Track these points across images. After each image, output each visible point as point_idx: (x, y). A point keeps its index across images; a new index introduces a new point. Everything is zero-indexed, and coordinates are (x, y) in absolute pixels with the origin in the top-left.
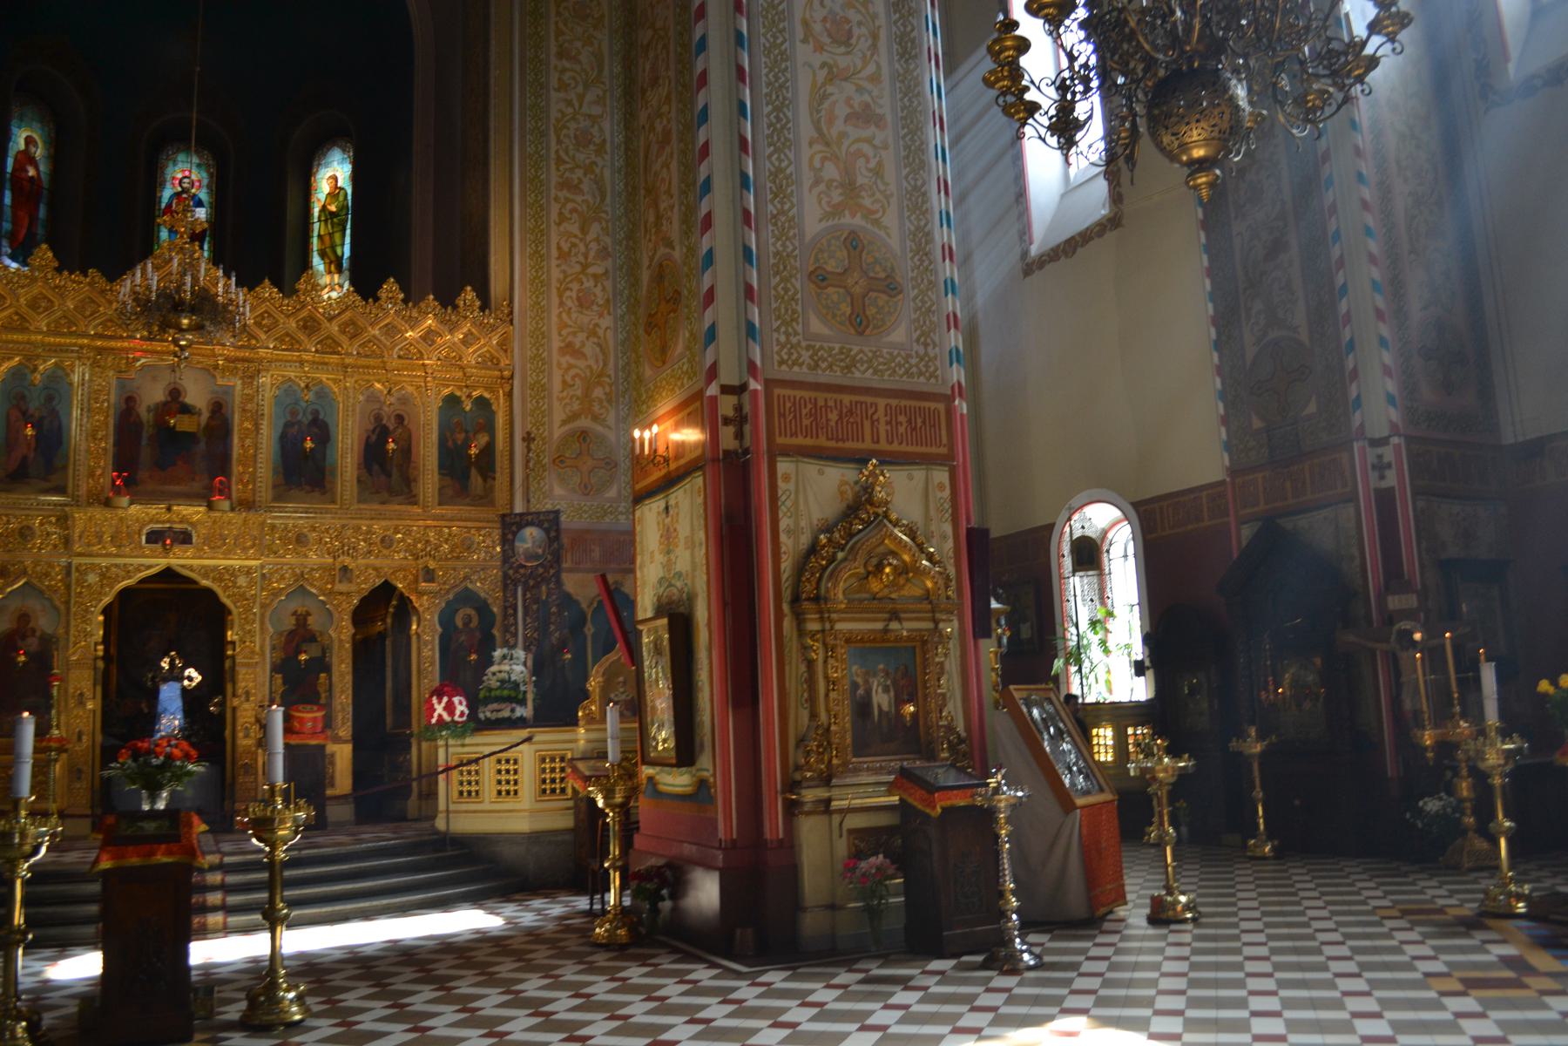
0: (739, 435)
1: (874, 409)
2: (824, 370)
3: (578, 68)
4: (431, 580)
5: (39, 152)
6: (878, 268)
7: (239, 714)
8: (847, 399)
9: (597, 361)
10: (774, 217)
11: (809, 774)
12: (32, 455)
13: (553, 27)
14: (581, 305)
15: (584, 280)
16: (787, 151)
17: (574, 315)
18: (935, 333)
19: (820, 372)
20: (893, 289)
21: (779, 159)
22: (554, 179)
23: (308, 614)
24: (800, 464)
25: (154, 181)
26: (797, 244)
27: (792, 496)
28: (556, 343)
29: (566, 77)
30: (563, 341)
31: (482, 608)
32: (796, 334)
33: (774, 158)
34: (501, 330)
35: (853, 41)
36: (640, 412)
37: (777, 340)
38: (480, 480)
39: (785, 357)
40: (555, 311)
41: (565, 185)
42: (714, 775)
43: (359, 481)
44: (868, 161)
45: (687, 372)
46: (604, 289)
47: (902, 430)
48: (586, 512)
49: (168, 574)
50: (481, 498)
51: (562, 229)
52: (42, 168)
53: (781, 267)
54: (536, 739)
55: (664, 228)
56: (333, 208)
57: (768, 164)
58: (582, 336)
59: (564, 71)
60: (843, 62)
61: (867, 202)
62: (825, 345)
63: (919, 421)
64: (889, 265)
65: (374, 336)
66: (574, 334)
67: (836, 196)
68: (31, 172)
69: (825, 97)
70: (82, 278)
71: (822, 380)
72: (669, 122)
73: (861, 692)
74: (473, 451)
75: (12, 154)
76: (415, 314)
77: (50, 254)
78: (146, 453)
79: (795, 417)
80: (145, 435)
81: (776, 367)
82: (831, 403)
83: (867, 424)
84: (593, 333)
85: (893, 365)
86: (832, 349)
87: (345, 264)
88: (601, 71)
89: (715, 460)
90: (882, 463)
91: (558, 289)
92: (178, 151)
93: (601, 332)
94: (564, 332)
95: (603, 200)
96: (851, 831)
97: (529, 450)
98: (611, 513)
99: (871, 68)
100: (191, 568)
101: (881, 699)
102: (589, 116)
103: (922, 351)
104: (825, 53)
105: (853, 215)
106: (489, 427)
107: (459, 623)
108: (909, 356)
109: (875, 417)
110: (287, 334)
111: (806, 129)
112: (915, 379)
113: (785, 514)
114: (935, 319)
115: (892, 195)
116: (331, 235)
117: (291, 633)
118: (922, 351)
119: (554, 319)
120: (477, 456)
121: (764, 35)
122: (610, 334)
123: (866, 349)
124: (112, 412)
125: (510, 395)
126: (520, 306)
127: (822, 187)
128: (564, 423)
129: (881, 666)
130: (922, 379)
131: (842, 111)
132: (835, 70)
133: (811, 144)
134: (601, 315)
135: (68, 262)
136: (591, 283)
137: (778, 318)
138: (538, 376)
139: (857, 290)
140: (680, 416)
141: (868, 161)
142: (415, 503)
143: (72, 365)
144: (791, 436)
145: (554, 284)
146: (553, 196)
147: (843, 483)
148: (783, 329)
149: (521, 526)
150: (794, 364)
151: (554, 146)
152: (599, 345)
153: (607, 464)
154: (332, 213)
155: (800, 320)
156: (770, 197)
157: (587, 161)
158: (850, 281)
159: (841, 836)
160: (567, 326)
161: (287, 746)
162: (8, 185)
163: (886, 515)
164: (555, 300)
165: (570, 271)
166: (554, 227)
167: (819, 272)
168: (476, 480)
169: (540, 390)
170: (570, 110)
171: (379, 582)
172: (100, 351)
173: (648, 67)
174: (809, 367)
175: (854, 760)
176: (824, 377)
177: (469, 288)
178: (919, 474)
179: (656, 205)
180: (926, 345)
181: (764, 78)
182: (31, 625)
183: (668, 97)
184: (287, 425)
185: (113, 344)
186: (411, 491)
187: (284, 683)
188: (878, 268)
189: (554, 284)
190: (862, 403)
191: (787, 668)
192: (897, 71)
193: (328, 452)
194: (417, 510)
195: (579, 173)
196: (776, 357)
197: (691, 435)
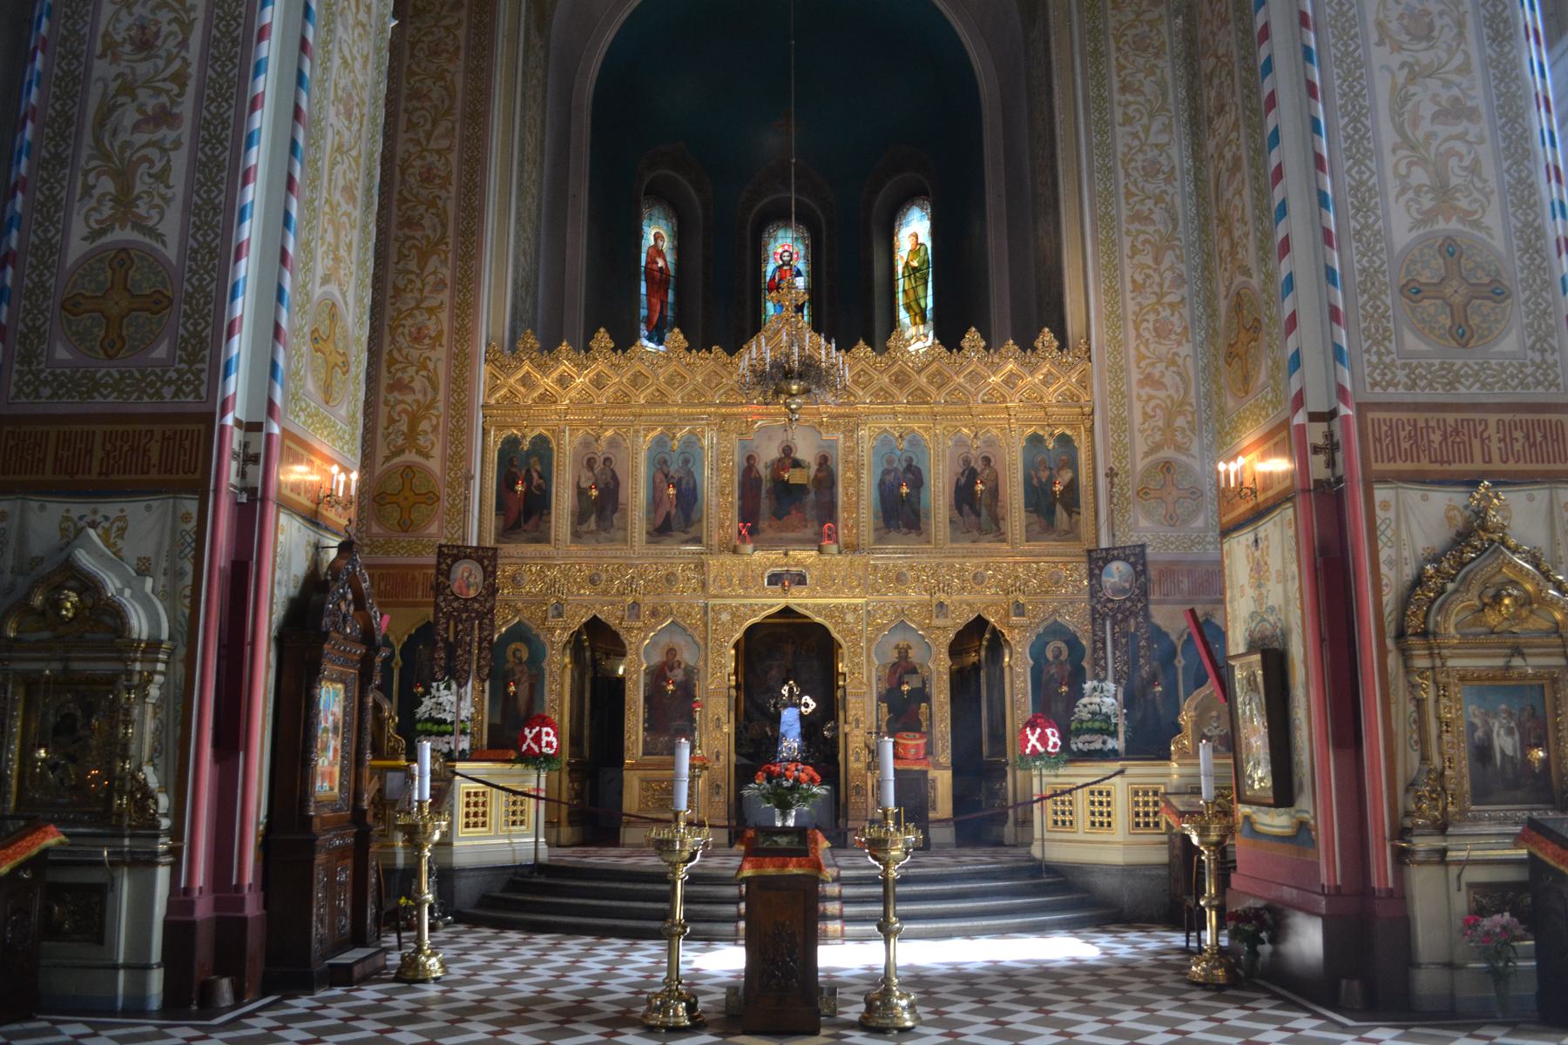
0: (1331, 463)
1: (1483, 427)
2: (1423, 389)
3: (1141, 99)
4: (1022, 614)
5: (666, 245)
6: (1480, 273)
7: (850, 739)
8: (1451, 418)
9: (1177, 391)
10: (1358, 232)
11: (1420, 821)
12: (673, 511)
13: (1114, 63)
14: (1158, 336)
15: (1160, 309)
16: (1367, 162)
17: (1152, 347)
18: (1553, 337)
19: (1418, 391)
20: (1499, 294)
21: (1360, 172)
22: (1125, 213)
23: (909, 647)
24: (1400, 490)
25: (758, 259)
26: (1384, 257)
27: (1393, 525)
28: (1135, 376)
30: (1142, 373)
31: (1073, 642)
32: (1389, 352)
34: (1079, 368)
35: (1436, 34)
36: (1225, 444)
37: (1368, 361)
38: (1065, 515)
39: (1379, 378)
40: (1132, 344)
41: (1137, 217)
42: (1315, 818)
43: (951, 522)
44: (1461, 158)
45: (1271, 401)
47: (1517, 446)
48: (1172, 543)
49: (787, 611)
50: (1067, 533)
51: (1135, 261)
52: (669, 259)
53: (1369, 285)
54: (1128, 772)
55: (1240, 256)
56: (915, 264)
57: (1348, 179)
58: (1161, 366)
59: (1128, 104)
60: (1425, 58)
61: (1463, 203)
62: (1423, 361)
63: (1539, 439)
64: (1493, 268)
65: (959, 384)
66: (1153, 365)
67: (1427, 202)
68: (661, 263)
69: (1407, 98)
70: (707, 355)
71: (1421, 399)
72: (1238, 147)
73: (1479, 733)
74: (1058, 488)
75: (644, 249)
76: (996, 360)
77: (681, 337)
78: (765, 505)
79: (1392, 441)
81: (1368, 390)
82: (1433, 423)
83: (1476, 443)
84: (1172, 363)
85: (1504, 376)
86: (1432, 365)
87: (929, 315)
88: (1165, 99)
89: (1306, 491)
90: (1496, 484)
91: (1134, 322)
92: (778, 228)
93: (1180, 361)
94: (1143, 364)
95: (1175, 228)
96: (1471, 886)
97: (1112, 485)
98: (1199, 543)
99: (1458, 59)
101: (1504, 743)
102: (1157, 145)
103: (1538, 358)
104: (1405, 53)
105: (1448, 220)
106: (1073, 464)
107: (1050, 656)
108: (1524, 365)
109: (1485, 435)
110: (881, 389)
111: (1387, 135)
112: (1532, 391)
113: (1385, 544)
114: (1552, 322)
115: (1492, 192)
116: (914, 289)
118: (1538, 358)
119: (1132, 352)
120: (1062, 492)
121: (1335, 46)
123: (1471, 362)
124: (736, 470)
125: (1091, 430)
126: (1097, 342)
127: (1410, 194)
128: (1147, 454)
129: (1503, 706)
130: (1540, 389)
131: (1428, 110)
132: (1417, 68)
133: (1394, 151)
134: (1179, 344)
135: (699, 341)
136: (1168, 312)
137: (1368, 338)
138: (1118, 409)
139: (1458, 299)
140: (1266, 446)
141: (1461, 158)
142: (1004, 541)
143: (703, 431)
144: (1389, 461)
145: (1131, 317)
146: (1124, 230)
147: (1451, 508)
148: (1374, 349)
149: (1107, 561)
150: (1389, 384)
152: (1179, 374)
153: (1193, 493)
154: (914, 269)
155: (1393, 337)
156: (1351, 212)
157: (1157, 191)
158: (1448, 291)
159: (1459, 890)
160: (1144, 357)
162: (643, 277)
163: (1503, 542)
164: (1132, 333)
165: (1145, 303)
166: (1127, 261)
167: (1412, 284)
168: (1061, 514)
169: (1121, 424)
170: (1136, 143)
171: (972, 617)
172: (725, 417)
173: (1213, 94)
174: (1406, 387)
175: (1473, 807)
176: (1422, 396)
177: (1046, 330)
178: (1541, 494)
179: (1230, 232)
180: (1543, 351)
181: (1338, 90)
182: (678, 658)
183: (1236, 126)
184: (886, 472)
185: (735, 410)
186: (999, 529)
187: (889, 712)
188: (1480, 273)
189: (1131, 317)
190: (1468, 420)
191: (1393, 707)
192: (1490, 57)
193: (922, 496)
194: (1005, 547)
195: (1150, 203)
196: (1368, 380)
197: (1280, 465)
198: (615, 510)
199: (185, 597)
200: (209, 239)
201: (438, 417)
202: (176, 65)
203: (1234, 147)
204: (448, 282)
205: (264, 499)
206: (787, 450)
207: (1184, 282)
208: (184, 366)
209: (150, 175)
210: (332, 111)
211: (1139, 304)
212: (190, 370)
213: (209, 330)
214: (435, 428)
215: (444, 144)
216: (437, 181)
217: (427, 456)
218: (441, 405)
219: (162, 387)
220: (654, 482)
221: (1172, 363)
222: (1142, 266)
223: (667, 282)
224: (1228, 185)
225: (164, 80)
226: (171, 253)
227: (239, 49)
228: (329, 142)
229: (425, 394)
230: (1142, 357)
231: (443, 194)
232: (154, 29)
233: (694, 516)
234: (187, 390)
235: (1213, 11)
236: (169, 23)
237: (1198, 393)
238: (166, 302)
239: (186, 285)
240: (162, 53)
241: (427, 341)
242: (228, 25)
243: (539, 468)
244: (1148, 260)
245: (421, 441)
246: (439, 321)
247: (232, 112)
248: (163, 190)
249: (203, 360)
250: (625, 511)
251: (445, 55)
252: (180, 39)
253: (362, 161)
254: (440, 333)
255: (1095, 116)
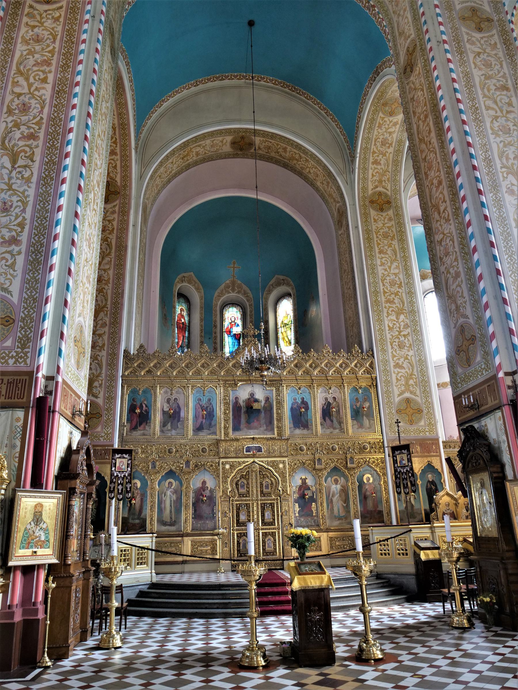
3: (387, 256)
4: (353, 463)
5: (185, 314)
13: (375, 242)
14: (400, 348)
17: (398, 352)
22: (383, 299)
25: (222, 320)
28: (392, 364)
29: (383, 261)
33: (512, 276)
41: (388, 301)
45: (484, 368)
46: (408, 340)
55: (462, 311)
56: (285, 322)
57: (511, 279)
58: (402, 360)
59: (382, 258)
66: (399, 359)
68: (183, 321)
72: (458, 268)
80: (243, 411)
84: (406, 358)
88: (396, 256)
93: (409, 358)
94: (395, 359)
100: (262, 462)
117: (300, 487)
122: (413, 358)
128: (399, 395)
134: (409, 351)
136: (403, 338)
145: (389, 340)
151: (382, 288)
152: (409, 363)
160: (395, 356)
161: (362, 535)
164: (390, 347)
165: (394, 335)
166: (385, 318)
168: (366, 422)
170: (386, 273)
173: (442, 248)
183: (456, 260)
189: (389, 340)
193: (309, 413)
195: (393, 296)
198: (179, 421)
199: (16, 457)
200: (33, 294)
201: (102, 380)
202: (20, 219)
203: (456, 269)
204: (108, 323)
205: (54, 411)
206: (252, 395)
207: (409, 326)
208: (19, 350)
209: (6, 266)
210: (85, 243)
211: (392, 335)
212: (22, 352)
213: (32, 334)
214: (101, 385)
215: (107, 267)
216: (104, 282)
217: (97, 397)
218: (103, 375)
219: (8, 359)
220: (196, 409)
221: (406, 358)
222: (392, 320)
223: (186, 328)
224: (453, 283)
225: (14, 225)
226: (15, 299)
227: (49, 214)
228: (83, 257)
229: (97, 370)
230: (394, 356)
231: (106, 287)
232: (10, 204)
233: (213, 423)
234: (21, 361)
235: (441, 217)
236: (17, 202)
237: (417, 370)
238: (11, 321)
239: (22, 314)
240: (14, 215)
241: (98, 348)
242: (44, 204)
243: (145, 402)
244: (394, 318)
245: (94, 391)
246: (103, 340)
247: (45, 240)
248: (12, 271)
249: (29, 348)
250: (183, 421)
251: (108, 231)
252: (22, 208)
253: (93, 266)
254: (104, 345)
255: (370, 262)
